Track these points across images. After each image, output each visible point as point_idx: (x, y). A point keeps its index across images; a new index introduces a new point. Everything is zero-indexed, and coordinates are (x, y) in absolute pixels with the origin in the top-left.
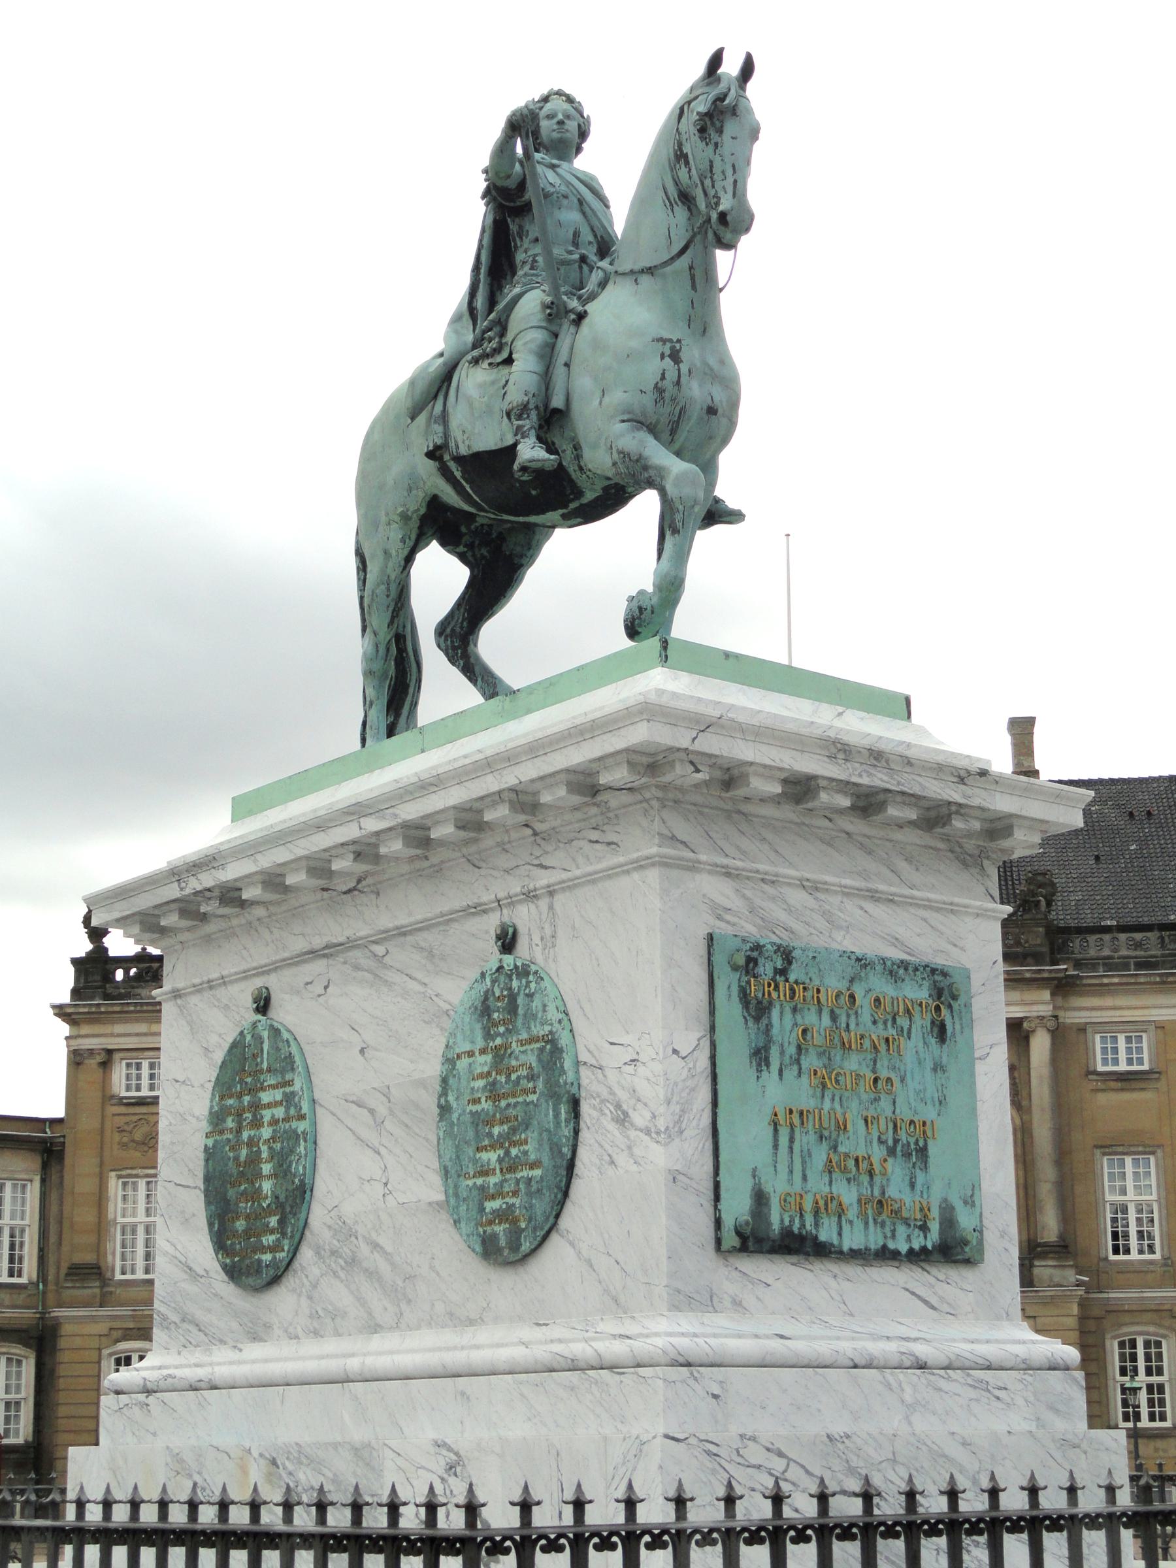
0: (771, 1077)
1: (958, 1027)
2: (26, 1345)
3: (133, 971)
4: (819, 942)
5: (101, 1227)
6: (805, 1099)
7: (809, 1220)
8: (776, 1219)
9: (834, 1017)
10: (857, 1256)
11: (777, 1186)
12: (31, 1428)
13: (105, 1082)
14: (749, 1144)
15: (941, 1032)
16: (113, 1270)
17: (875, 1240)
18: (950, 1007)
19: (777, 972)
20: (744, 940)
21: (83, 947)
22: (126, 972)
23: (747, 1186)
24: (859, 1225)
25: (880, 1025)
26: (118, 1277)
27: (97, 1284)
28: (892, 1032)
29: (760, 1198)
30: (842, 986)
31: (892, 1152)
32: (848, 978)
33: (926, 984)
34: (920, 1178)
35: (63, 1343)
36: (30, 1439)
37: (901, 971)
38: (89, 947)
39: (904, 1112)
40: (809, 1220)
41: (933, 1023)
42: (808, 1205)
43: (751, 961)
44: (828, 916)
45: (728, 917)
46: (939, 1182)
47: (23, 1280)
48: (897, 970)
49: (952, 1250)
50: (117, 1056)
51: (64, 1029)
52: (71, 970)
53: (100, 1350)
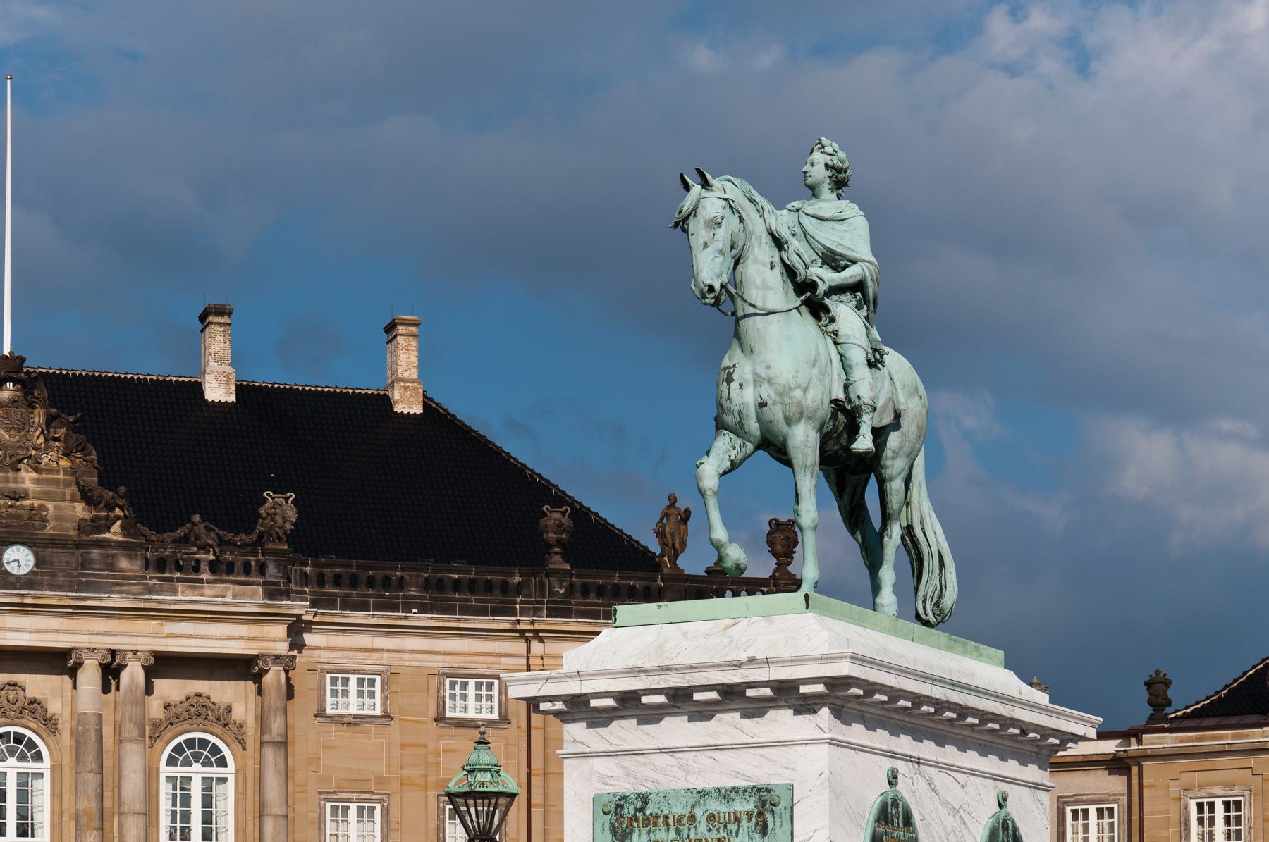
1: (778, 824)
4: (681, 785)
9: (678, 832)
15: (764, 830)
18: (772, 811)
19: (637, 810)
20: (614, 795)
25: (714, 831)
28: (723, 834)
30: (686, 811)
32: (690, 805)
33: (753, 799)
37: (733, 795)
41: (757, 824)
43: (619, 807)
44: (686, 769)
45: (611, 782)
48: (726, 795)
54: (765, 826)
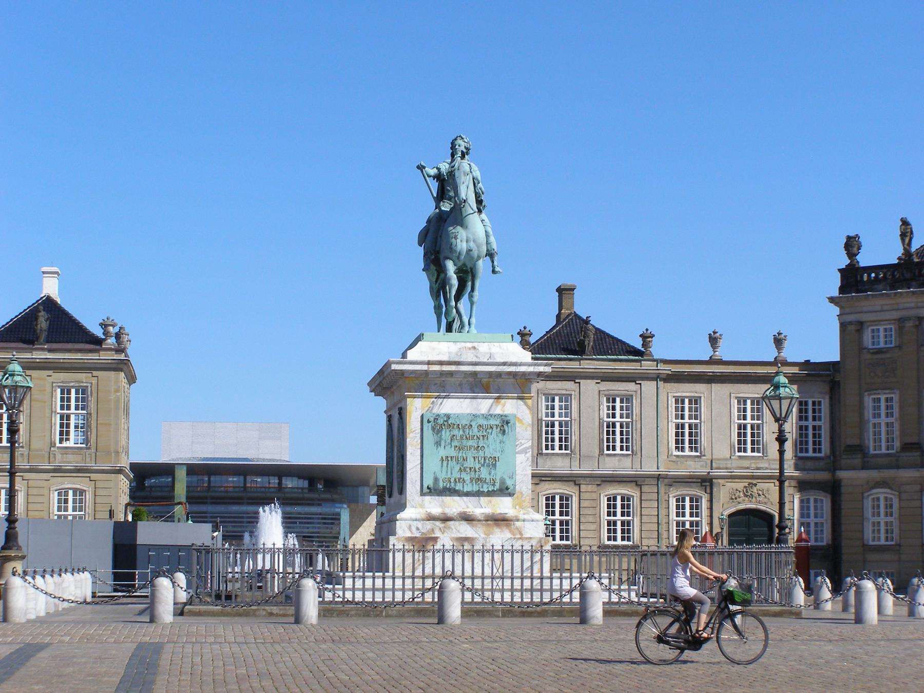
0: (441, 449)
2: (825, 491)
3: (873, 275)
5: (862, 423)
6: (452, 452)
7: (453, 485)
8: (441, 485)
9: (464, 431)
10: (467, 494)
11: (442, 476)
12: (830, 537)
13: (860, 340)
14: (433, 466)
15: (504, 432)
16: (869, 448)
17: (475, 488)
21: (845, 261)
22: (869, 276)
23: (432, 476)
24: (470, 485)
26: (872, 452)
27: (860, 456)
28: (485, 433)
29: (436, 480)
30: (468, 423)
31: (483, 465)
34: (493, 472)
35: (843, 490)
36: (830, 542)
38: (847, 261)
39: (488, 455)
40: (453, 485)
42: (452, 480)
46: (500, 472)
47: (822, 455)
49: (504, 491)
50: (865, 325)
51: (836, 310)
52: (838, 276)
53: (863, 494)
54: (504, 431)
